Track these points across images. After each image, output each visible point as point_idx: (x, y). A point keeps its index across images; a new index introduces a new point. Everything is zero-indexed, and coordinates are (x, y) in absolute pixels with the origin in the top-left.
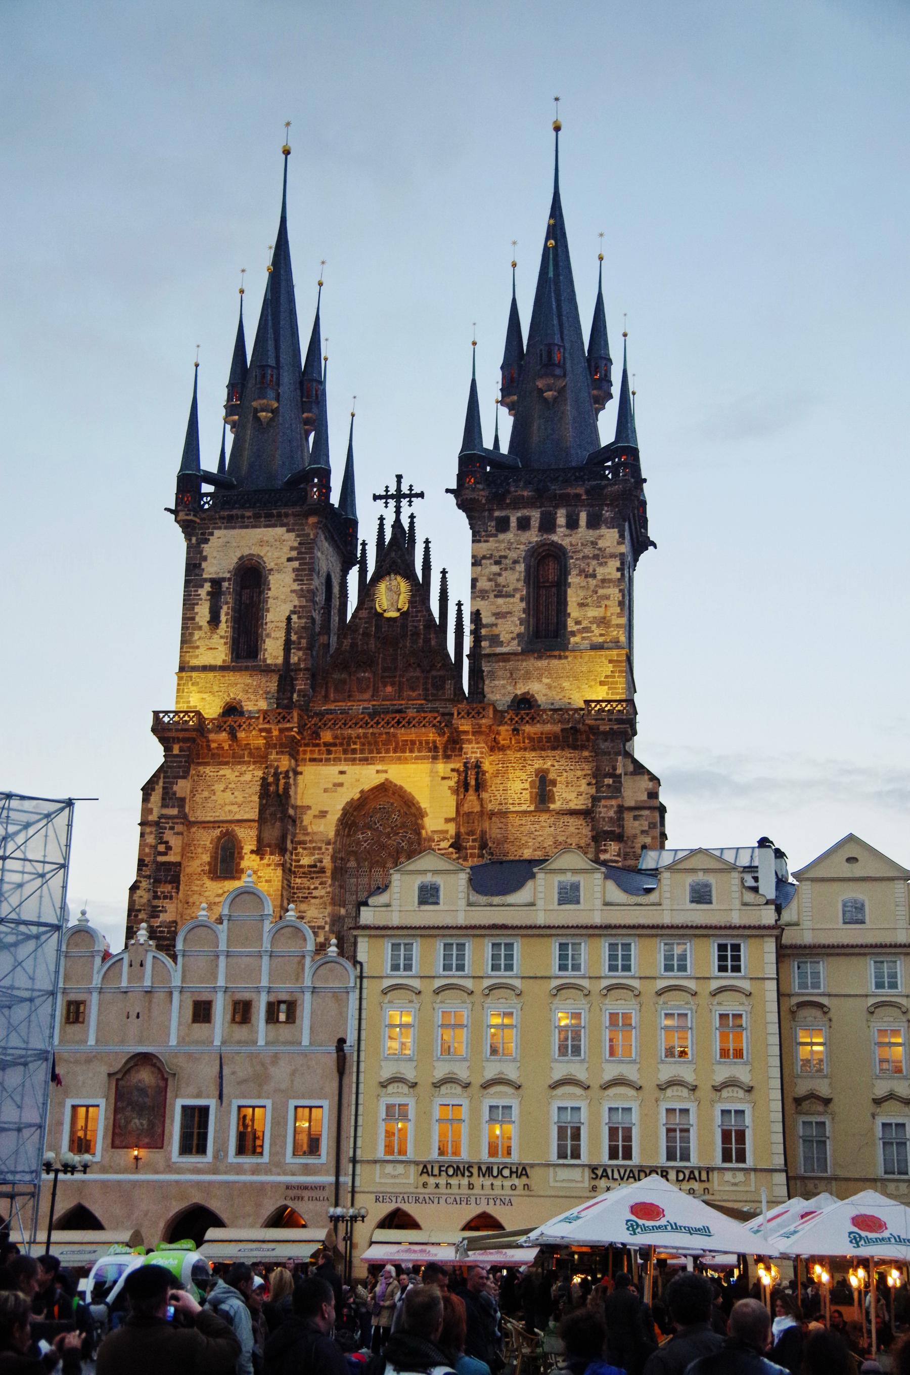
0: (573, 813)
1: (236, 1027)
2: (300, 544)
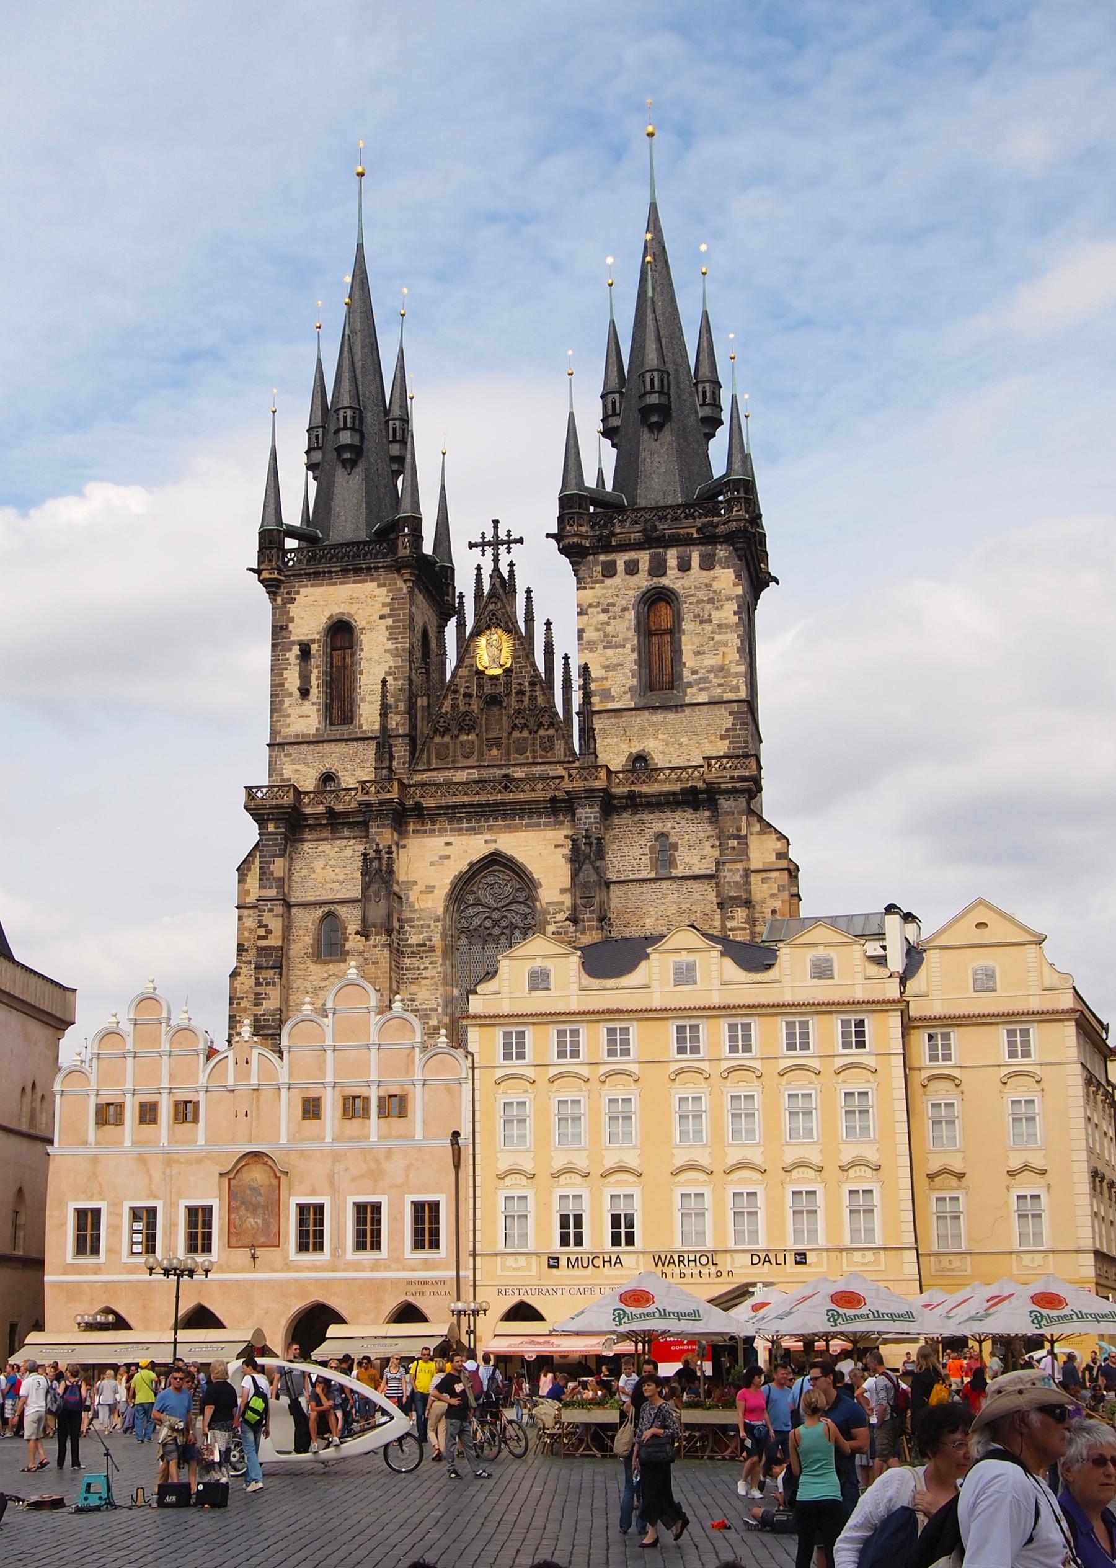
0: (696, 877)
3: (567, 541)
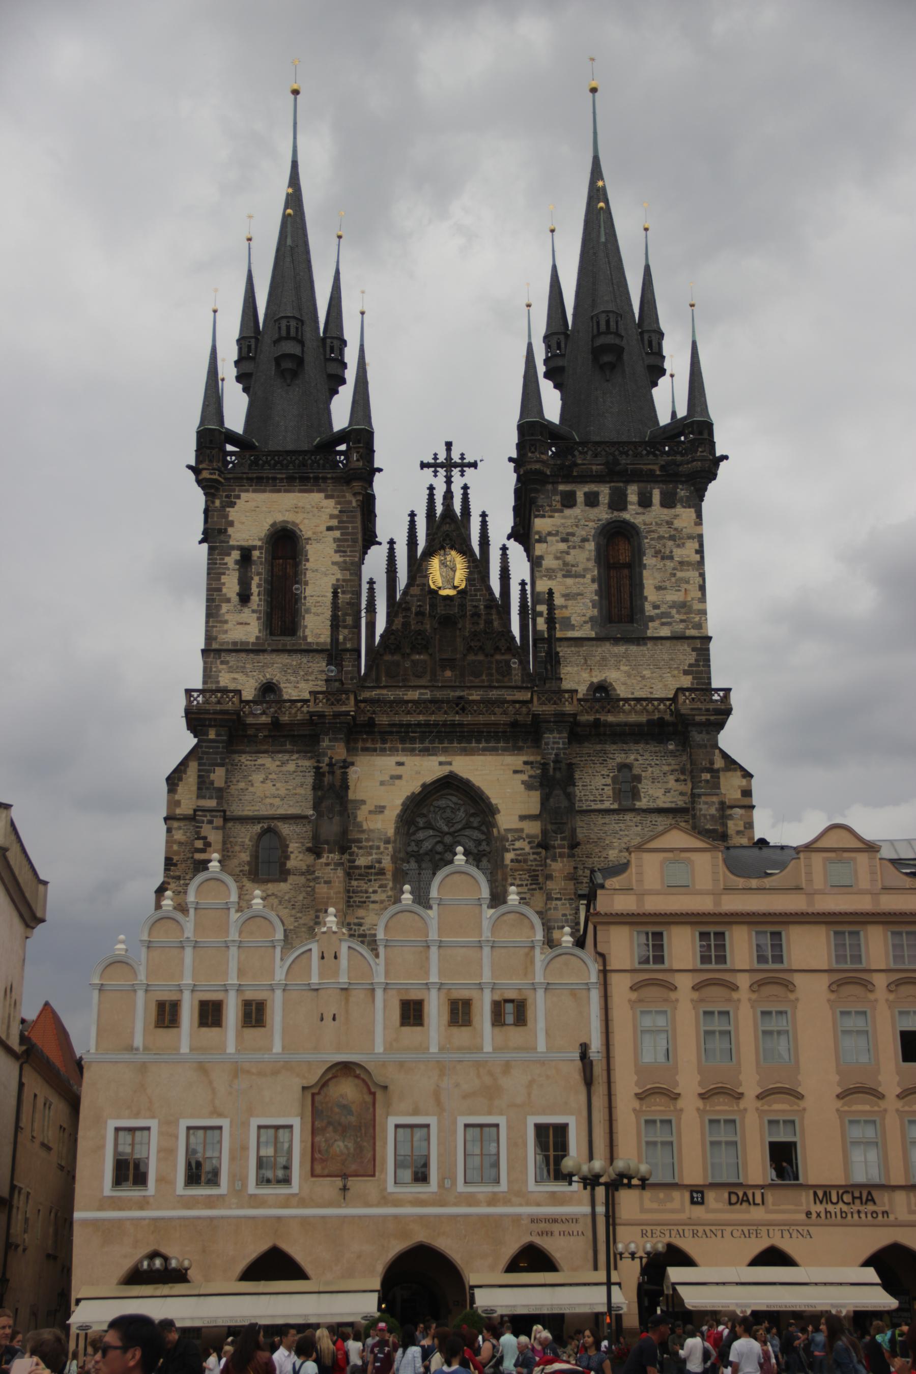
1: (455, 1030)
2: (340, 512)
3: (529, 467)
